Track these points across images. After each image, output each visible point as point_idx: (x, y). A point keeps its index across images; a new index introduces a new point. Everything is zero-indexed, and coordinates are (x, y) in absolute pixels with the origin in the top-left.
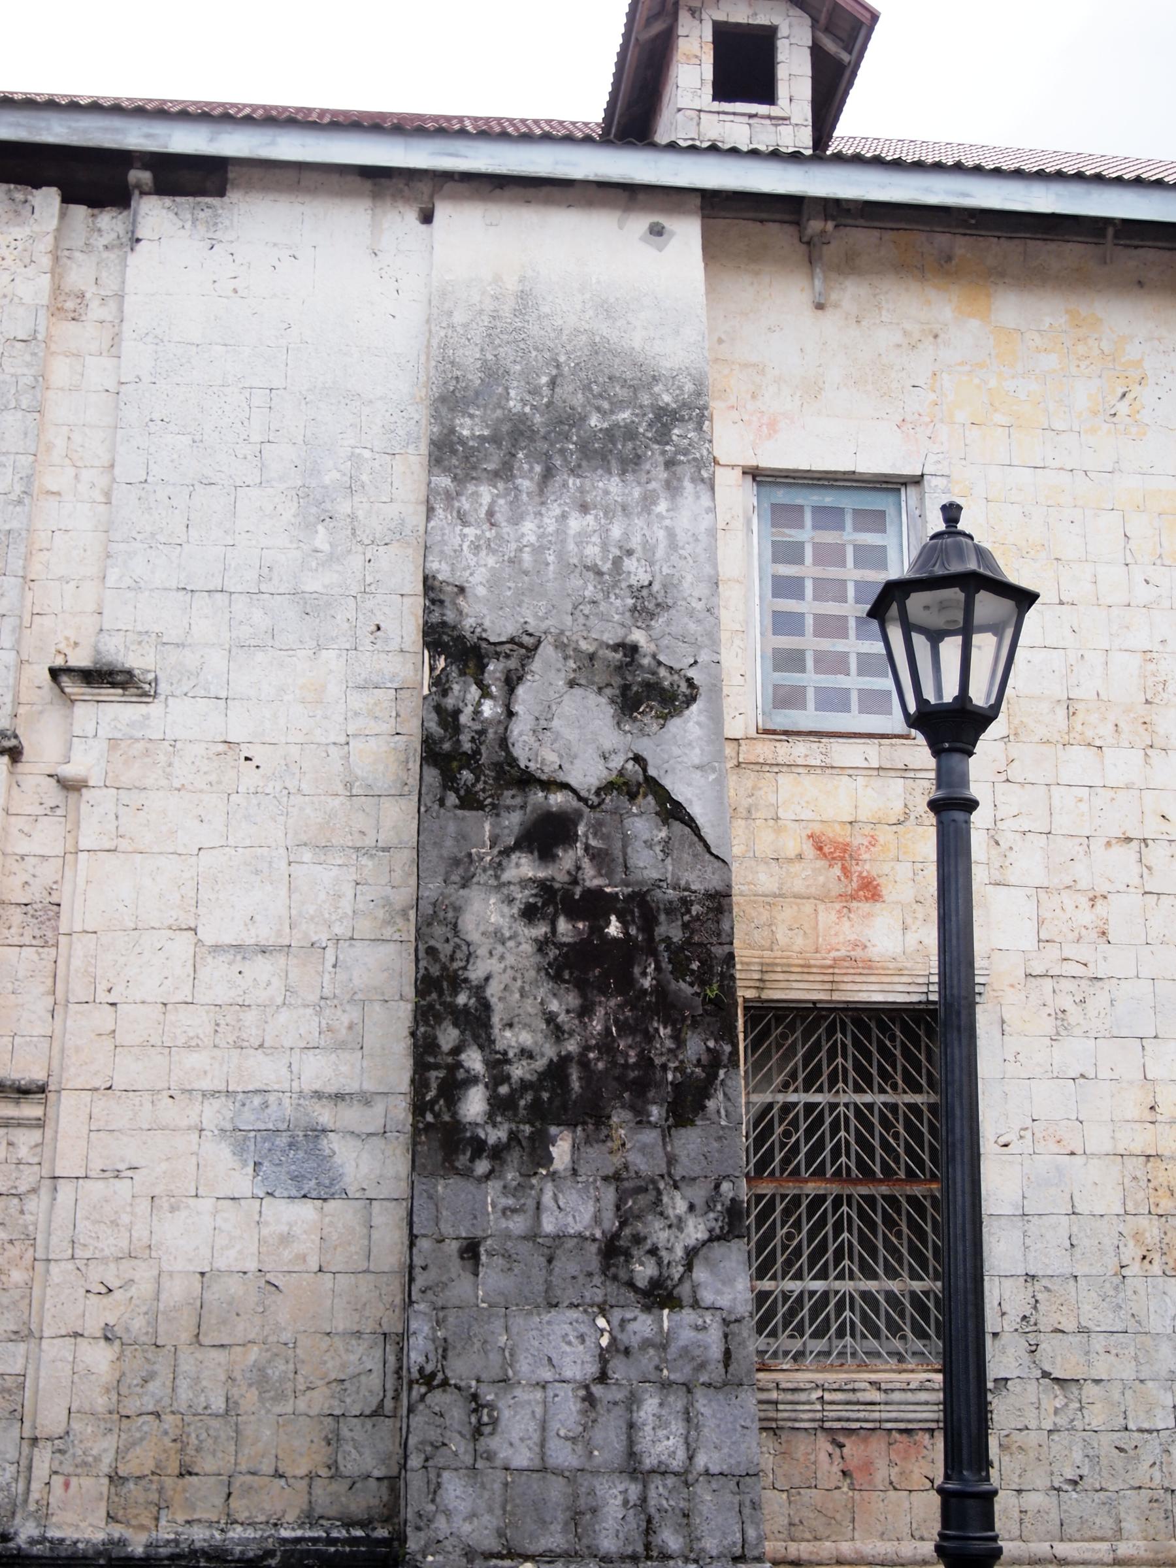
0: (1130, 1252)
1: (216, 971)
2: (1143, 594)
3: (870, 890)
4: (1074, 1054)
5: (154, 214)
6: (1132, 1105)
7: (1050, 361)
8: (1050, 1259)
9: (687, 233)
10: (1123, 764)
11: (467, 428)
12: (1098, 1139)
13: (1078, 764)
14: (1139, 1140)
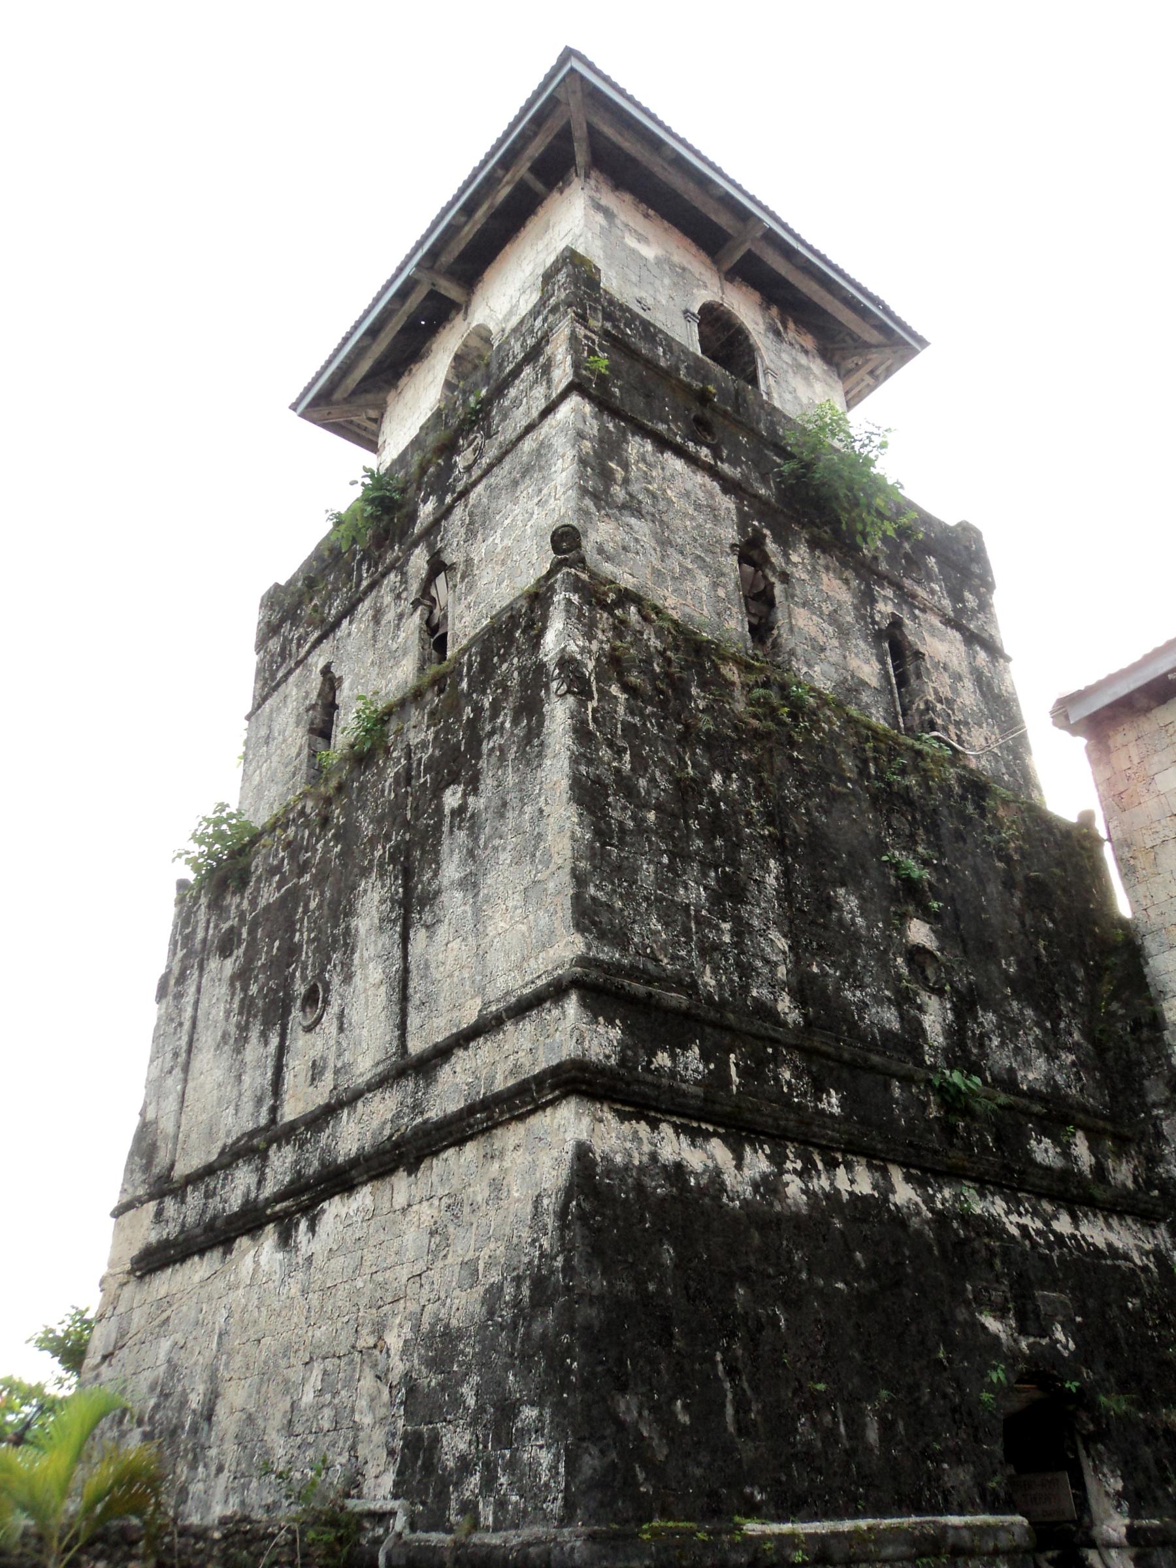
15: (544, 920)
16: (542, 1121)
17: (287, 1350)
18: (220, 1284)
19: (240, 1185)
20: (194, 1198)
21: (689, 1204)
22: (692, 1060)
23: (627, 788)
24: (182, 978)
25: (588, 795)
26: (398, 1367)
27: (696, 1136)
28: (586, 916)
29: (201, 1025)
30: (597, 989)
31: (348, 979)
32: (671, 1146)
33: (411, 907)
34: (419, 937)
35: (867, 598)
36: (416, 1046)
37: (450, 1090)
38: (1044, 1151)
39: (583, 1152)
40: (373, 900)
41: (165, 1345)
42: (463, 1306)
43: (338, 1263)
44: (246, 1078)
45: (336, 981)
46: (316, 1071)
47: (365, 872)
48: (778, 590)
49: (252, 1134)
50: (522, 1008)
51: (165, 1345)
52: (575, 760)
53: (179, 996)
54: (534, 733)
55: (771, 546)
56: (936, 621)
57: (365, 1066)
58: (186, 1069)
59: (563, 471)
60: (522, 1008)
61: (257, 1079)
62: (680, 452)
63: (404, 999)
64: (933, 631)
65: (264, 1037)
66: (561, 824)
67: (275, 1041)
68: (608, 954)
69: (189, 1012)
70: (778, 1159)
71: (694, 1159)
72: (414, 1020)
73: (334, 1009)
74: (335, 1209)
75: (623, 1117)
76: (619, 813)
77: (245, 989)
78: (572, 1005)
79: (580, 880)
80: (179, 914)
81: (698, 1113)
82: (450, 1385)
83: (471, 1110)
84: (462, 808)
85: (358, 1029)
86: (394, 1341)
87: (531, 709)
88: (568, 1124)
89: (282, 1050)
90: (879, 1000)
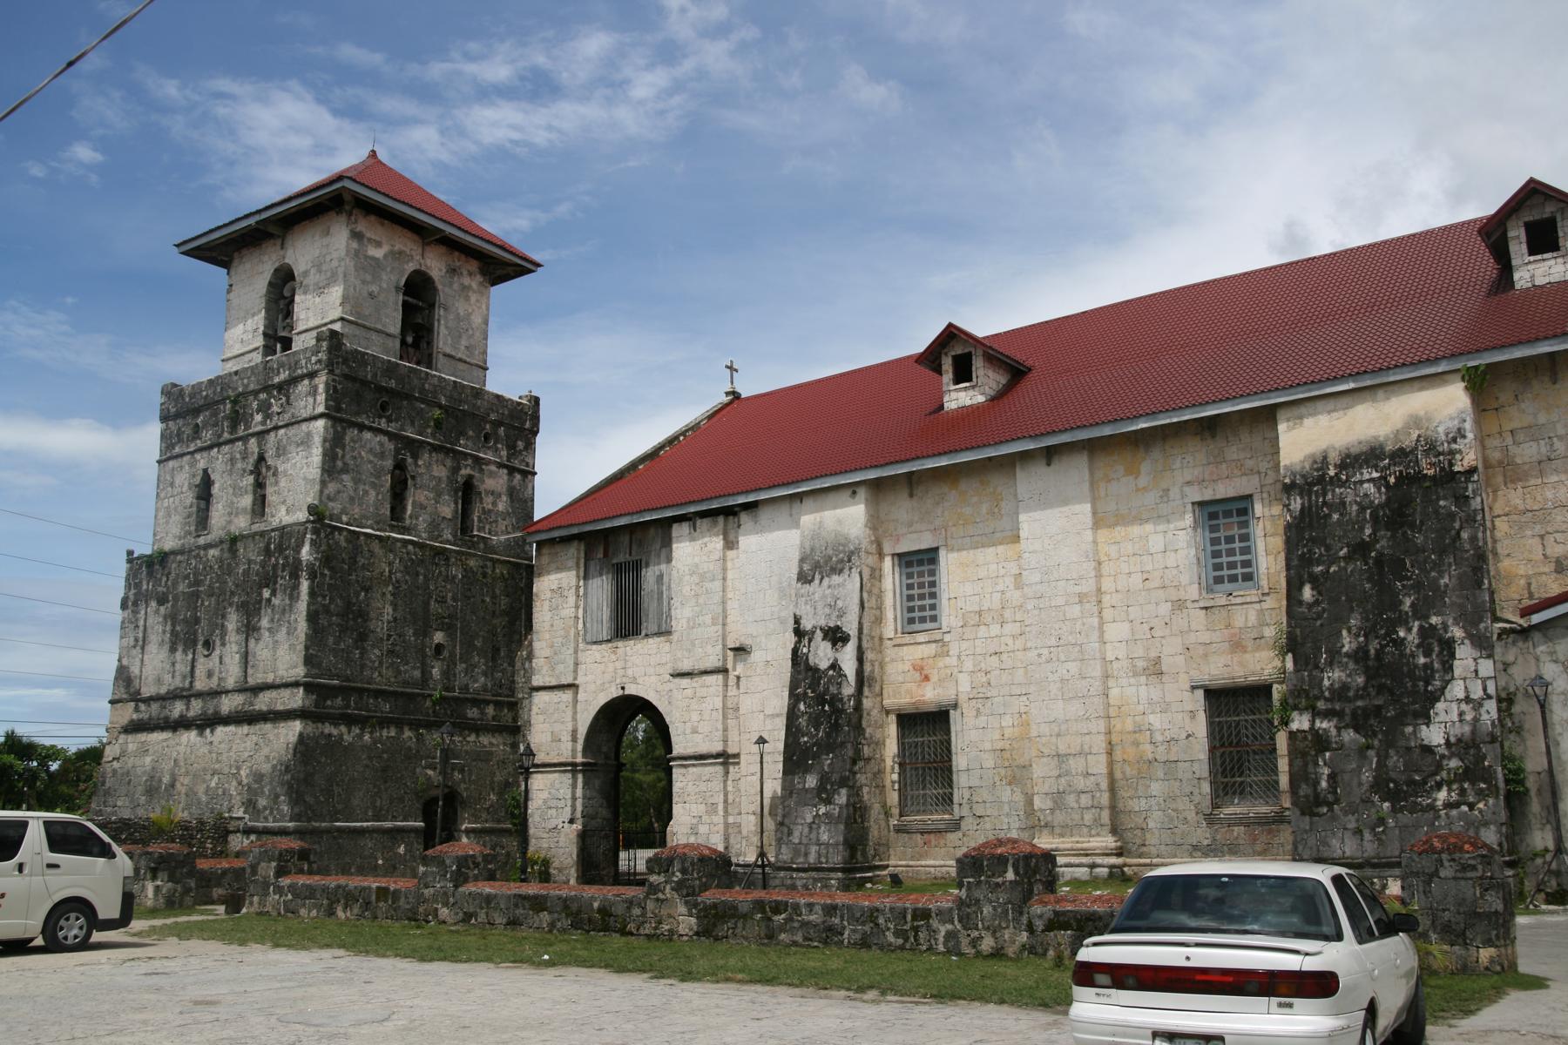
0: (997, 779)
1: (768, 722)
2: (1002, 572)
3: (927, 678)
4: (982, 721)
5: (744, 517)
6: (997, 736)
7: (975, 499)
8: (975, 782)
9: (862, 493)
10: (995, 629)
11: (806, 567)
12: (988, 746)
13: (982, 631)
14: (1000, 745)
16: (290, 723)
17: (205, 770)
18: (172, 742)
19: (178, 709)
20: (155, 706)
21: (332, 745)
22: (339, 701)
23: (327, 611)
24: (135, 604)
25: (312, 617)
26: (245, 781)
27: (336, 725)
28: (309, 660)
30: (309, 688)
31: (223, 645)
32: (328, 729)
33: (250, 629)
34: (252, 643)
35: (455, 470)
36: (251, 681)
37: (263, 702)
38: (472, 713)
39: (301, 734)
40: (233, 621)
41: (148, 760)
42: (266, 768)
44: (178, 666)
45: (218, 643)
46: (210, 675)
47: (231, 605)
48: (410, 482)
49: (183, 689)
50: (286, 685)
51: (148, 760)
52: (308, 605)
53: (135, 612)
54: (296, 587)
55: (410, 460)
56: (493, 468)
57: (230, 683)
58: (143, 648)
59: (316, 454)
60: (286, 685)
61: (183, 668)
62: (370, 429)
63: (246, 662)
64: (492, 475)
65: (185, 651)
66: (302, 626)
68: (315, 671)
69: (141, 623)
70: (362, 729)
71: (335, 732)
72: (250, 671)
73: (217, 652)
74: (220, 730)
76: (323, 621)
77: (173, 625)
78: (301, 690)
79: (307, 648)
80: (130, 569)
81: (335, 720)
82: (262, 788)
83: (270, 712)
84: (269, 600)
86: (242, 773)
87: (295, 576)
88: (297, 726)
89: (194, 660)
90: (414, 668)
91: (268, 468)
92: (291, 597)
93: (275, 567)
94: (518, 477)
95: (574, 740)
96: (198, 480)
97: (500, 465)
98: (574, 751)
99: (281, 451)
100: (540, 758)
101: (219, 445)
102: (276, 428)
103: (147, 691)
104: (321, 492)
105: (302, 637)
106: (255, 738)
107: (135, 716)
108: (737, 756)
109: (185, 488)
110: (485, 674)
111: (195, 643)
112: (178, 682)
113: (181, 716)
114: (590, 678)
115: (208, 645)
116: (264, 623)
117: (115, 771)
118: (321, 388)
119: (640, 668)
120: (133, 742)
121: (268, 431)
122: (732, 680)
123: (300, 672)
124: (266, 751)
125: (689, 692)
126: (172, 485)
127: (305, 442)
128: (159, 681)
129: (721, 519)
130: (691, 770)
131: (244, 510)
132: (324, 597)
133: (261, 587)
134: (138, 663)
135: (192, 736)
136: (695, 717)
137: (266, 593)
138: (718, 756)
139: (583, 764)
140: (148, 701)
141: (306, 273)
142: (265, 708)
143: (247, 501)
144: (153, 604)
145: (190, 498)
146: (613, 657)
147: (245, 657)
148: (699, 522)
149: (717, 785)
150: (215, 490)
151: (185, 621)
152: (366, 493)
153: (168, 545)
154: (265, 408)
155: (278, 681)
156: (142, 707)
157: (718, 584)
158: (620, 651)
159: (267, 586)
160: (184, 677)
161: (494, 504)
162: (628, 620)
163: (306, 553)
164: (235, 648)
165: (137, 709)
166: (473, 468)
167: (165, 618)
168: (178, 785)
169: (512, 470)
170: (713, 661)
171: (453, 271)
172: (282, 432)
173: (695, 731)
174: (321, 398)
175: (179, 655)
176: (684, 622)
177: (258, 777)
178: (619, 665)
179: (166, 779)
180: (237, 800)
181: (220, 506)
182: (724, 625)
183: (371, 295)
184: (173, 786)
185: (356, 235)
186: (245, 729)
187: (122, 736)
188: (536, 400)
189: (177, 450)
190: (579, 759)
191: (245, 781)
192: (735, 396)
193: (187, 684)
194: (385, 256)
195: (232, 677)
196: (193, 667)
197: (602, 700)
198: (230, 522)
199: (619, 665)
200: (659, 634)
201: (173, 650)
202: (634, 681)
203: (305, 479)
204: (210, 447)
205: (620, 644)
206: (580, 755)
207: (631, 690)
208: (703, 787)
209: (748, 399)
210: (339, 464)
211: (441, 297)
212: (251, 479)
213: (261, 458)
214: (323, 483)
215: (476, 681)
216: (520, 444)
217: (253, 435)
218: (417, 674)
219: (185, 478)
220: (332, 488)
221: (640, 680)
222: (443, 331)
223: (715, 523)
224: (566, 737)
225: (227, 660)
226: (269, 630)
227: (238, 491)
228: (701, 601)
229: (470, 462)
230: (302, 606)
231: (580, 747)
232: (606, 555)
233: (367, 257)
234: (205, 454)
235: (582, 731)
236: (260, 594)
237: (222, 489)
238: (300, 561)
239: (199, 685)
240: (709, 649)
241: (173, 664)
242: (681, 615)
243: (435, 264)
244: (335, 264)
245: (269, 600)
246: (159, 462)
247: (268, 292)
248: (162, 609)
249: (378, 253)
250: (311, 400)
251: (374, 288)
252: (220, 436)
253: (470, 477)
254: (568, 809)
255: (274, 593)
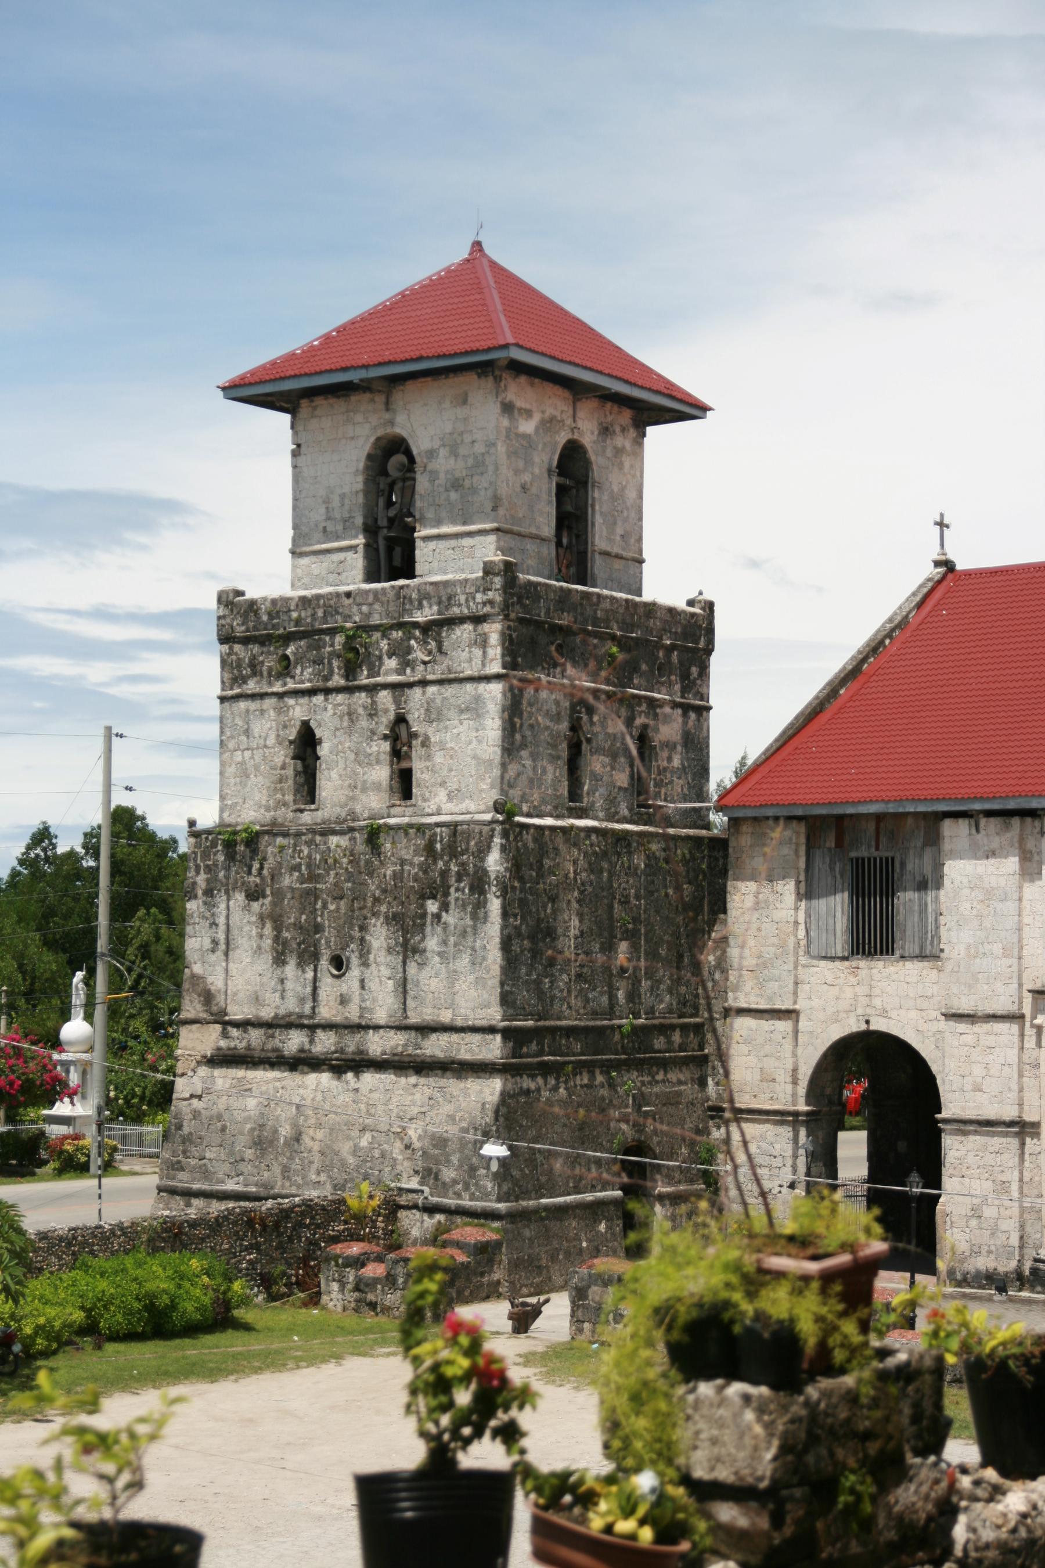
15: (485, 996)
19: (294, 1042)
23: (519, 935)
25: (506, 945)
27: (533, 1077)
28: (506, 1000)
29: (234, 932)
30: (507, 1034)
31: (365, 964)
33: (408, 949)
34: (412, 969)
36: (414, 1019)
37: (436, 1046)
41: (251, 1103)
43: (375, 1096)
44: (289, 985)
45: (355, 961)
46: (344, 1001)
49: (301, 1016)
51: (251, 1103)
54: (480, 905)
56: (667, 710)
58: (226, 954)
59: (493, 727)
63: (405, 992)
66: (494, 957)
67: (310, 975)
69: (221, 920)
70: (557, 1079)
75: (513, 1076)
76: (516, 948)
77: (278, 928)
78: (498, 1037)
79: (502, 984)
84: (438, 917)
85: (370, 988)
90: (601, 994)
91: (413, 736)
92: (474, 916)
93: (444, 874)
94: (693, 715)
95: (795, 1082)
96: (292, 734)
97: (675, 705)
98: (794, 1095)
99: (433, 714)
100: (743, 1101)
101: (327, 691)
102: (424, 683)
103: (236, 1013)
104: (502, 777)
105: (496, 970)
106: (428, 1092)
107: (223, 1043)
108: (1036, 1125)
109: (271, 741)
110: (670, 991)
111: (316, 957)
112: (291, 1005)
113: (302, 1050)
114: (816, 1002)
115: (339, 963)
116: (432, 943)
117: (196, 1114)
118: (494, 638)
119: (894, 999)
120: (224, 1078)
121: (411, 685)
122: (1030, 1032)
123: (494, 1014)
124: (447, 1109)
125: (969, 1039)
126: (247, 732)
127: (474, 709)
128: (257, 999)
129: (1016, 821)
130: (972, 1138)
131: (377, 787)
132: (515, 916)
133: (423, 897)
134: (220, 970)
135: (325, 1078)
136: (978, 1071)
137: (432, 907)
138: (1011, 1124)
139: (808, 1114)
140: (244, 1025)
141: (431, 454)
142: (441, 1055)
143: (382, 773)
144: (240, 897)
145: (282, 755)
146: (852, 980)
147: (403, 987)
148: (983, 821)
149: (1010, 1159)
150: (323, 750)
151: (298, 926)
152: (544, 771)
153: (251, 814)
154: (402, 652)
155: (459, 1022)
156: (234, 1032)
157: (1011, 906)
158: (863, 973)
159: (434, 897)
160: (302, 1000)
161: (670, 759)
162: (873, 936)
163: (494, 862)
164: (385, 972)
165: (225, 1035)
166: (647, 717)
167: (262, 918)
168: (306, 1140)
169: (686, 708)
170: (1003, 1004)
171: (606, 431)
172: (432, 689)
173: (978, 1088)
174: (495, 651)
175: (290, 969)
176: (962, 948)
177: (441, 1142)
178: (861, 990)
179: (285, 1131)
180: (405, 1166)
181: (334, 774)
182: (1020, 958)
183: (524, 488)
184: (297, 1138)
185: (508, 408)
186: (413, 1079)
187: (203, 1071)
188: (710, 606)
189: (252, 686)
190: (803, 1107)
191: (417, 1145)
192: (948, 565)
193: (307, 1009)
194: (537, 429)
195: (383, 1005)
196: (315, 989)
197: (836, 1033)
198: (353, 798)
199: (861, 990)
200: (922, 957)
201: (279, 960)
202: (884, 1013)
203: (475, 757)
204: (311, 692)
205: (863, 963)
206: (802, 1100)
207: (879, 1025)
208: (989, 1159)
209: (968, 574)
210: (518, 737)
211: (596, 473)
212: (386, 746)
213: (401, 719)
214: (504, 766)
215: (661, 1001)
216: (694, 671)
217: (385, 686)
218: (605, 999)
219: (270, 727)
220: (513, 769)
221: (893, 1014)
222: (599, 519)
223: (1008, 827)
224: (783, 1077)
225: (372, 985)
226: (439, 954)
227: (361, 758)
228: (987, 923)
229: (644, 707)
230: (493, 928)
231: (802, 1090)
232: (839, 844)
233: (517, 435)
234: (304, 700)
235: (806, 1071)
236: (423, 906)
237: (335, 751)
238: (485, 872)
239: (327, 1012)
240: (999, 988)
241: (282, 981)
242: (956, 937)
243: (586, 428)
244: (479, 448)
245: (438, 917)
246: (223, 699)
247: (367, 468)
248: (256, 906)
249: (527, 427)
250: (478, 652)
251: (527, 477)
252: (327, 679)
253: (645, 727)
254: (788, 1169)
255: (445, 907)
